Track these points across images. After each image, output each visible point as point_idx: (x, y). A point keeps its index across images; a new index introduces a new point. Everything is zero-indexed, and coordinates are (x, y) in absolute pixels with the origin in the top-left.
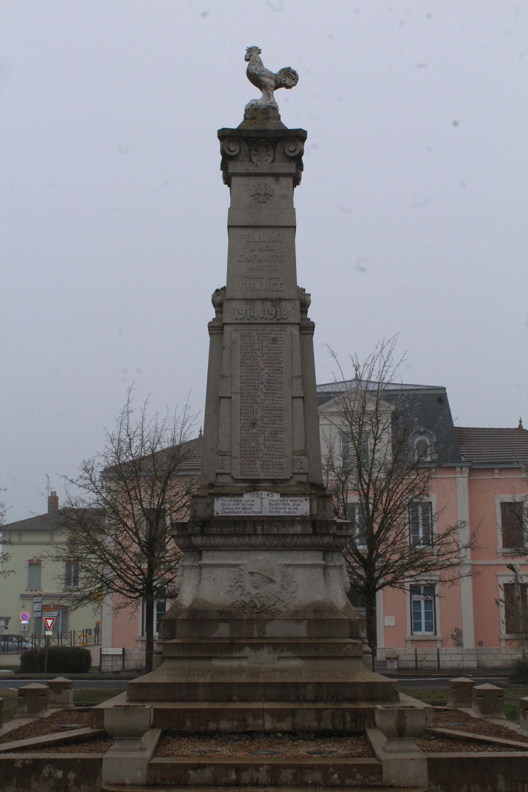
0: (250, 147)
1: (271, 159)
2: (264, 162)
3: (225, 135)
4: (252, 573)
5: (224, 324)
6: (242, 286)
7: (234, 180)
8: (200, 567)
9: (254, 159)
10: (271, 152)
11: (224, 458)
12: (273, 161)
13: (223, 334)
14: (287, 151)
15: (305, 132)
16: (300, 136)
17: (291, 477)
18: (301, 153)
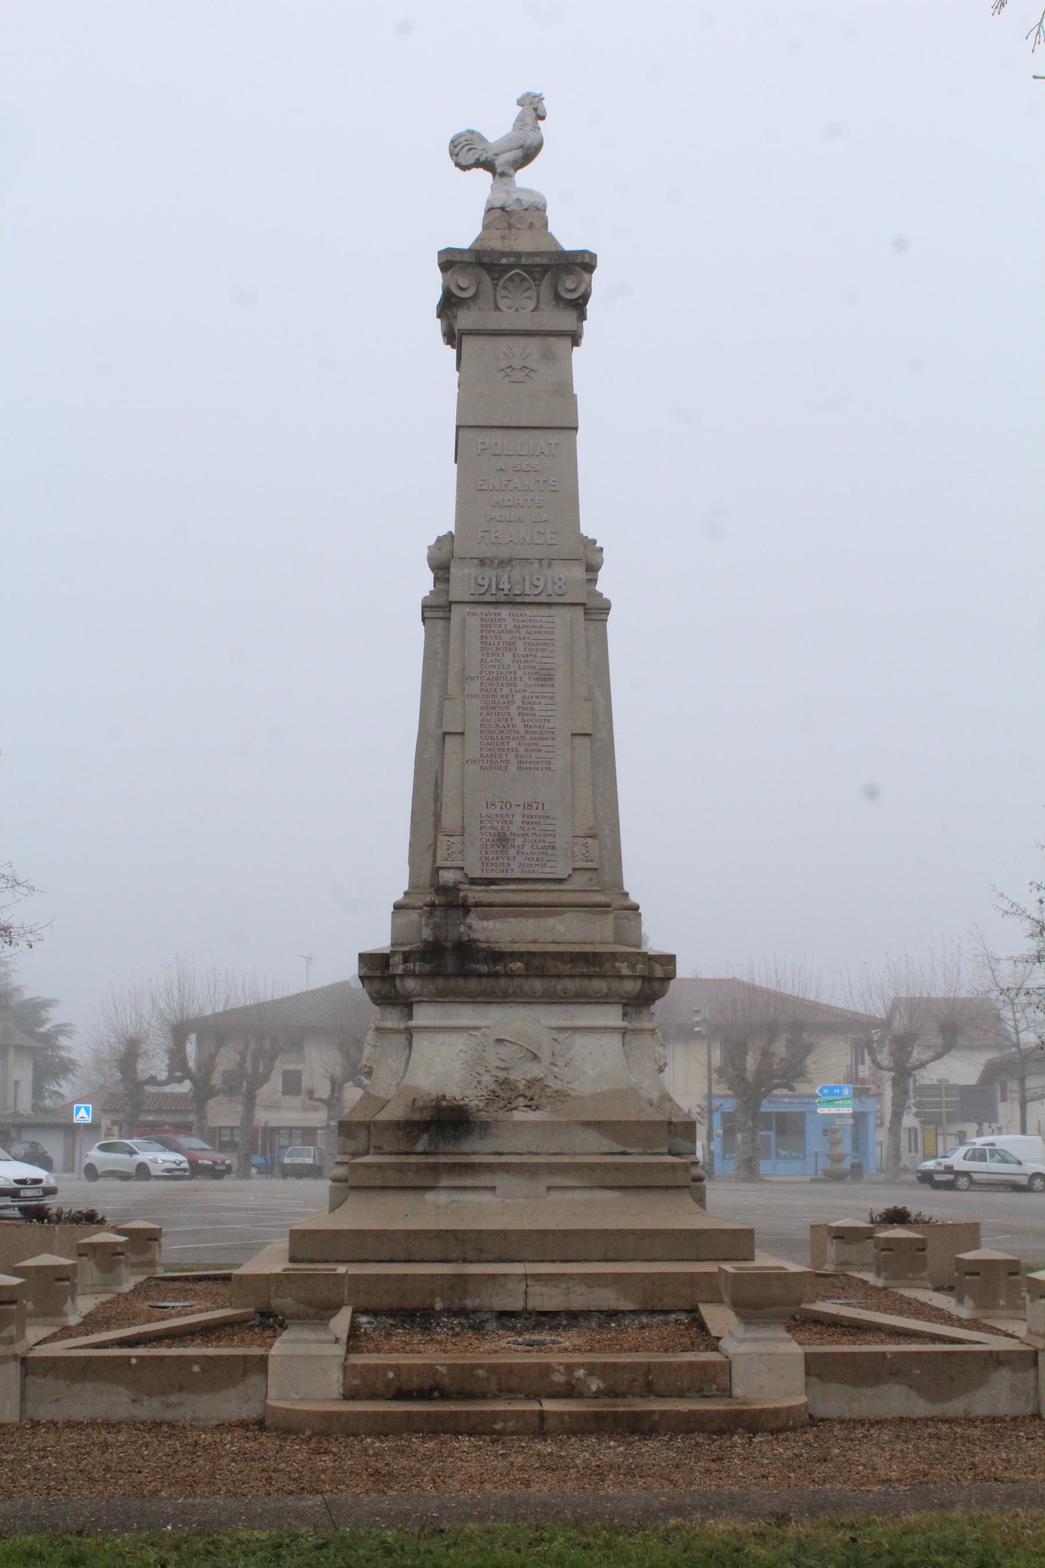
1: (532, 304)
2: (518, 308)
3: (450, 262)
4: (500, 1041)
5: (451, 603)
6: (483, 534)
8: (409, 1032)
9: (501, 304)
10: (533, 293)
11: (452, 839)
13: (449, 618)
15: (594, 257)
16: (583, 264)
17: (570, 875)
18: (585, 297)
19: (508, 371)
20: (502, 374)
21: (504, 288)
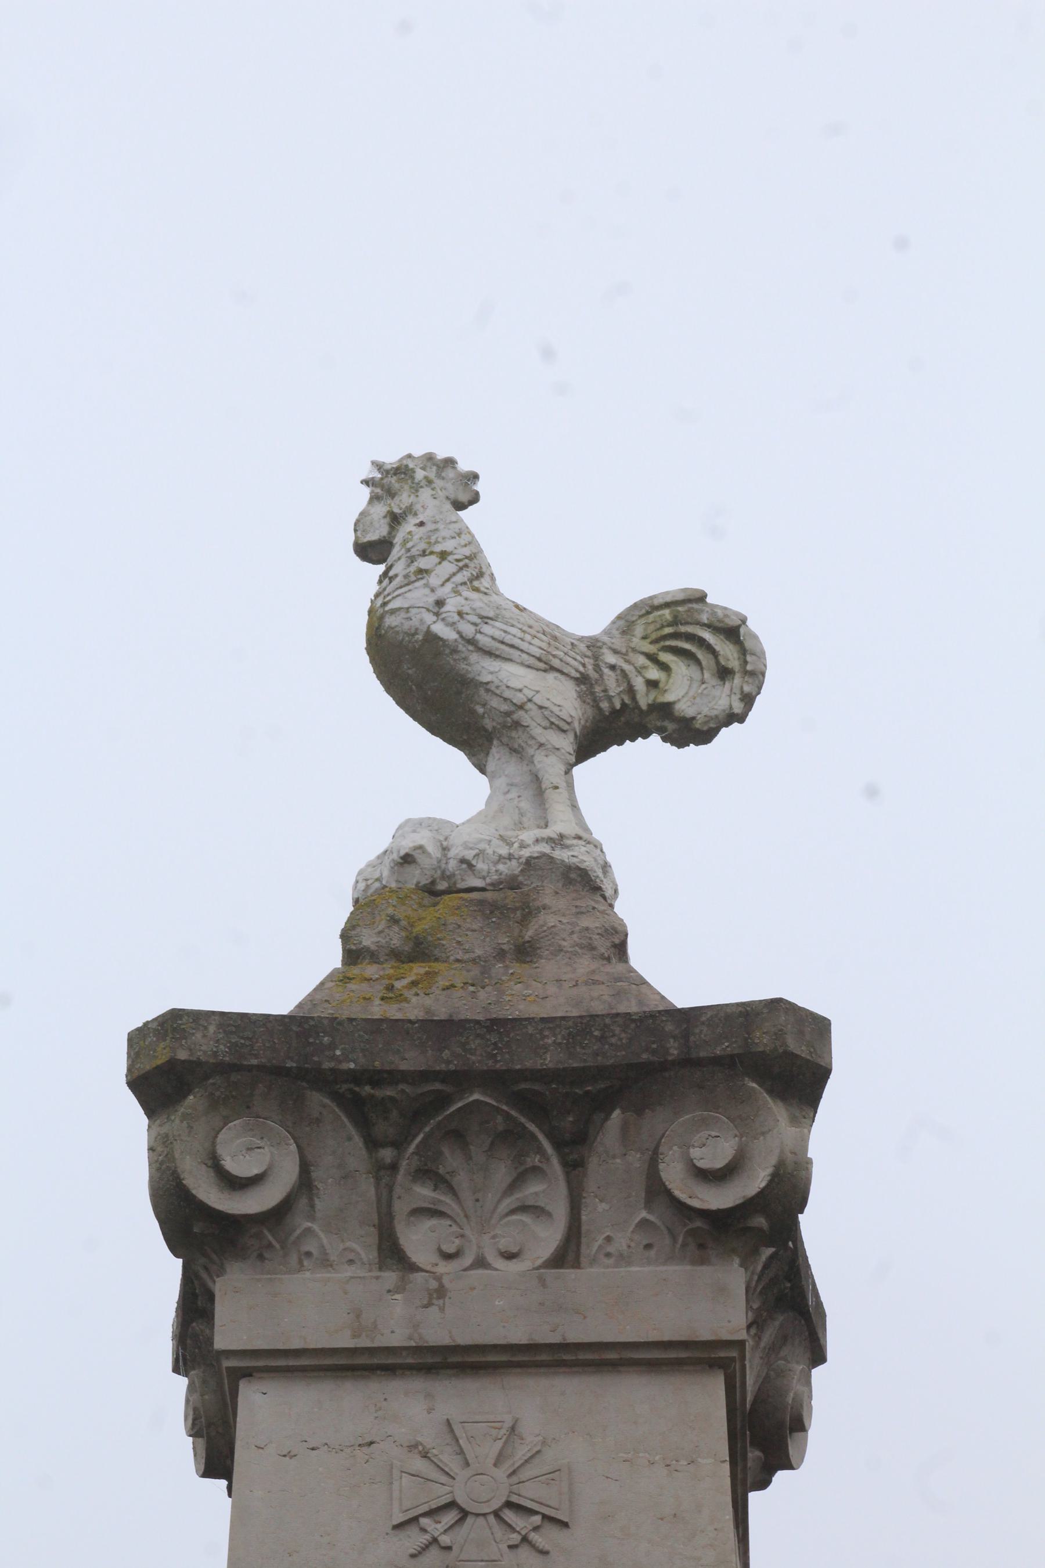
0: (387, 1154)
1: (548, 1237)
2: (494, 1259)
3: (185, 1068)
7: (258, 1407)
9: (419, 1240)
10: (550, 1190)
12: (567, 1255)
14: (673, 1175)
15: (818, 1028)
16: (775, 1059)
18: (789, 1191)
19: (434, 1527)
20: (415, 1539)
21: (427, 1173)
